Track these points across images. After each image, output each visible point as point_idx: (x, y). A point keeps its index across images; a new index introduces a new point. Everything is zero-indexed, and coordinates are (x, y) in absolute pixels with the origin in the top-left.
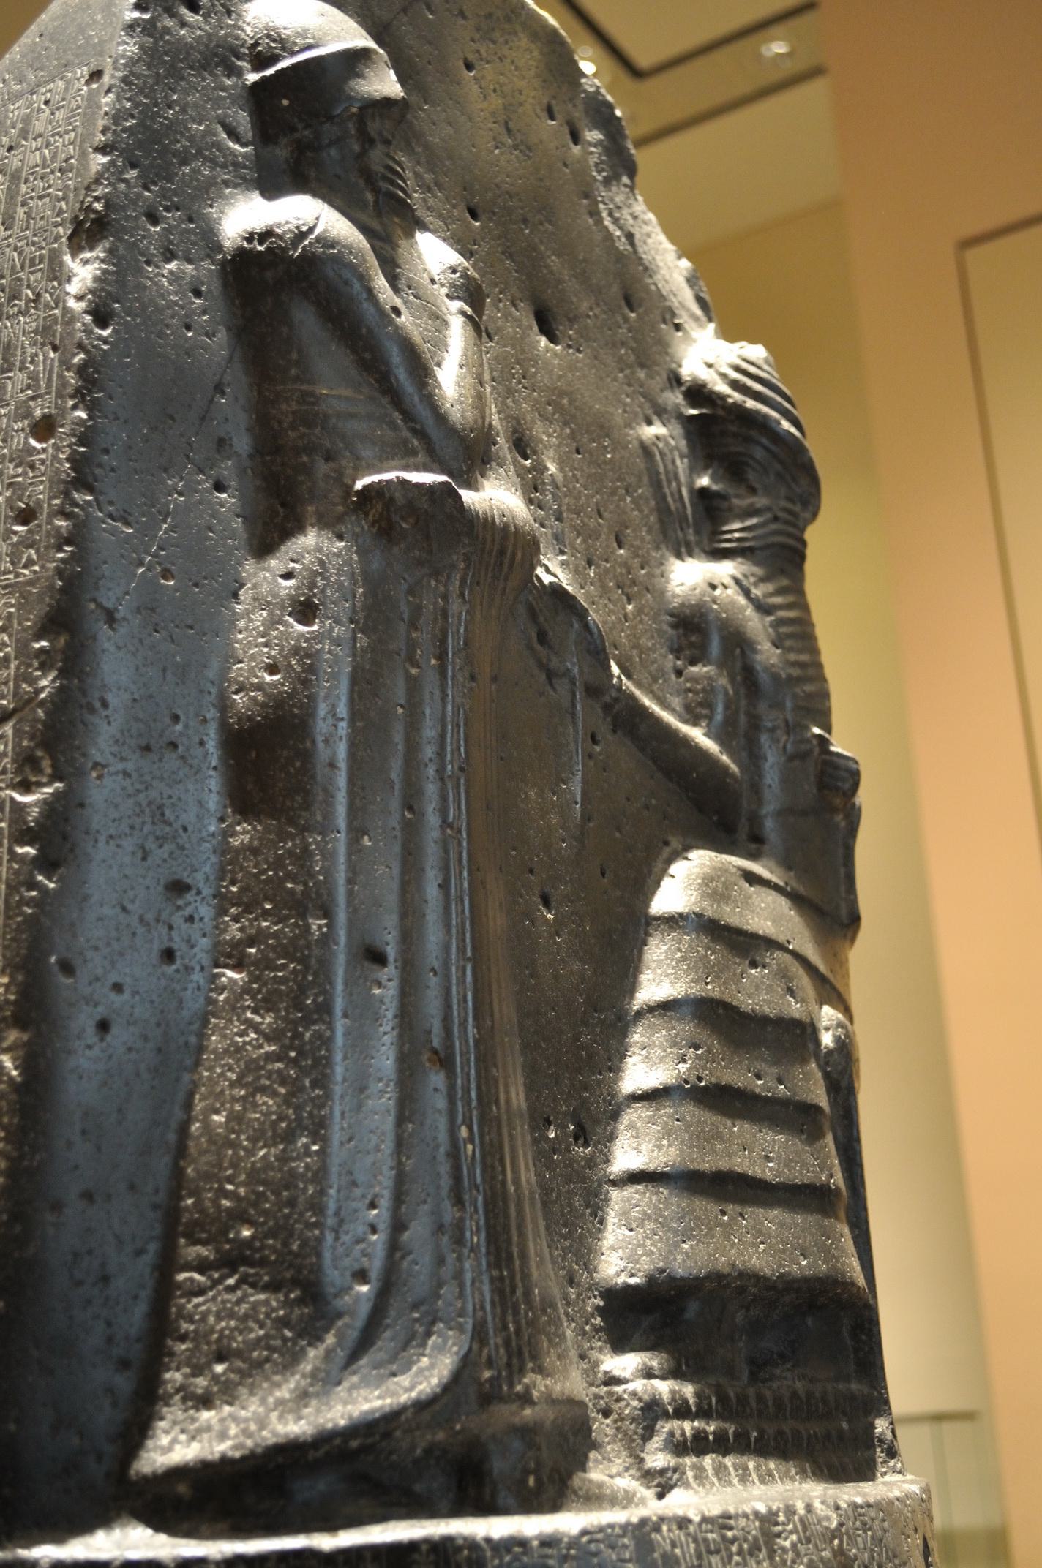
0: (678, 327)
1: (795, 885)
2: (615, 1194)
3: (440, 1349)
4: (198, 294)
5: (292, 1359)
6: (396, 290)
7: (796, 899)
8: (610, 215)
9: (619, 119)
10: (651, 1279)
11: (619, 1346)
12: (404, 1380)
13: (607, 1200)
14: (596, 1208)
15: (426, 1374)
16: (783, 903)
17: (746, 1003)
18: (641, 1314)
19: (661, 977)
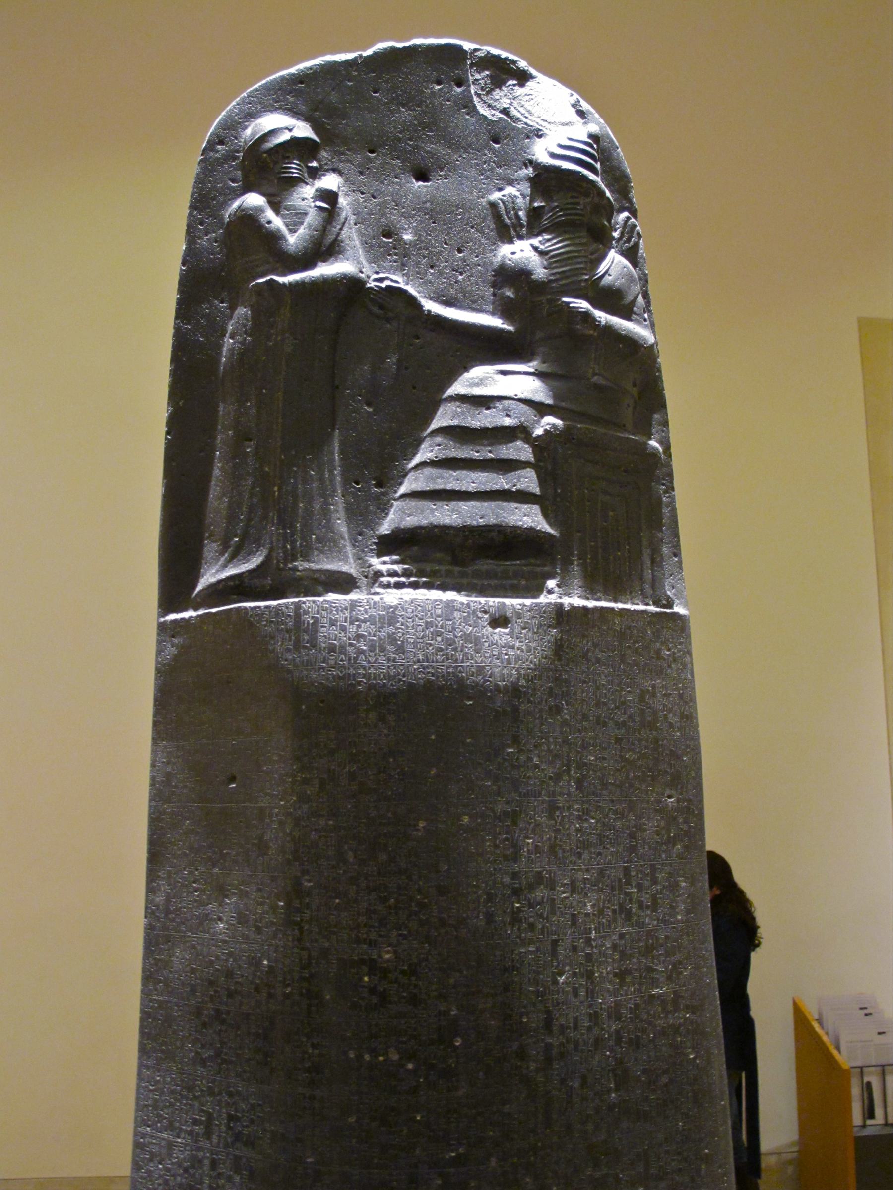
0: (540, 137)
1: (544, 368)
2: (395, 503)
3: (260, 555)
4: (216, 242)
5: (218, 560)
6: (277, 211)
7: (538, 374)
8: (489, 106)
9: (506, 59)
10: (393, 531)
11: (379, 556)
12: (246, 565)
13: (392, 505)
14: (384, 509)
15: (254, 562)
16: (531, 378)
17: (476, 424)
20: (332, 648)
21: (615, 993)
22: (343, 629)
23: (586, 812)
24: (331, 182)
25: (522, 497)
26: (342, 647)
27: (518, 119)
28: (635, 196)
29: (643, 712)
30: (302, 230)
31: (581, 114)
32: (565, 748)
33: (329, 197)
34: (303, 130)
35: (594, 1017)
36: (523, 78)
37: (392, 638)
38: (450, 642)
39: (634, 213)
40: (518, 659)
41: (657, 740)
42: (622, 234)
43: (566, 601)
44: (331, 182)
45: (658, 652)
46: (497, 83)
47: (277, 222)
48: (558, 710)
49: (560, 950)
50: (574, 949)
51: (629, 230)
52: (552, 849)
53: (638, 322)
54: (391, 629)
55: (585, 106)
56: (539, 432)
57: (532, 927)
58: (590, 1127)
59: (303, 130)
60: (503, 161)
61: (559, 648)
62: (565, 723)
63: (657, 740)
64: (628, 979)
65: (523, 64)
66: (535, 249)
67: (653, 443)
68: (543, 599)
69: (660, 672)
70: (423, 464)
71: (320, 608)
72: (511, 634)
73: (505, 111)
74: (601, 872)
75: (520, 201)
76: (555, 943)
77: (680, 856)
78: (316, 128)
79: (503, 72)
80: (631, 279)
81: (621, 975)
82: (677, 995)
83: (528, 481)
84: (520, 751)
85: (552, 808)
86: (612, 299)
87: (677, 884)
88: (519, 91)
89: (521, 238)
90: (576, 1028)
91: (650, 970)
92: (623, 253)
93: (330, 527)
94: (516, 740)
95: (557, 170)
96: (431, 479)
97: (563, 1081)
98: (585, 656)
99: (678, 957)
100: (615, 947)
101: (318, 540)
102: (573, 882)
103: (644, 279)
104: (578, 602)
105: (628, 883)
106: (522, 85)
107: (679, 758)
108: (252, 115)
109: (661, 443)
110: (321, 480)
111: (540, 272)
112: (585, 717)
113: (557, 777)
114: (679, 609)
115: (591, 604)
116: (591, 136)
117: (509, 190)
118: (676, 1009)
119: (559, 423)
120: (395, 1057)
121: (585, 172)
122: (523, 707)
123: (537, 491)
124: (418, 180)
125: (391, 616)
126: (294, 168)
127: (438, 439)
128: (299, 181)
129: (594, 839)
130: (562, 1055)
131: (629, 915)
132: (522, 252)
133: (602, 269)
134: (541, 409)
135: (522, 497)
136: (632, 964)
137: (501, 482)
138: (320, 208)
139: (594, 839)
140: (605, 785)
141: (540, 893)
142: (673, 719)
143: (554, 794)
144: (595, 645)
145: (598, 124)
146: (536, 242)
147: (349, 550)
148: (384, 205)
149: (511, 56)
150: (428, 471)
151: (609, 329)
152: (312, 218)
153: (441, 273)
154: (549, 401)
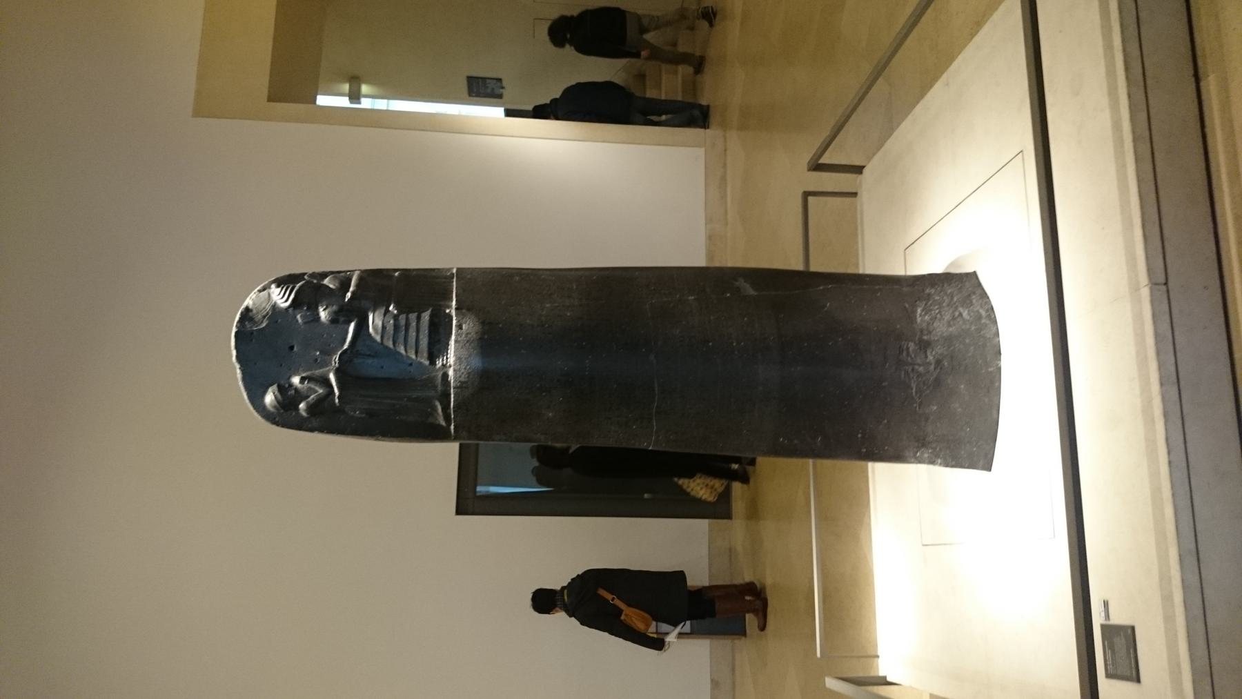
7: (374, 312)
14: (421, 363)
18: (432, 358)
19: (390, 344)
24: (296, 380)
25: (419, 318)
33: (302, 380)
46: (251, 319)
51: (313, 275)
61: (468, 310)
80: (335, 278)
83: (413, 316)
103: (332, 273)
104: (454, 303)
108: (264, 406)
111: (335, 308)
125: (459, 359)
128: (296, 390)
135: (419, 318)
137: (414, 324)
151: (357, 286)
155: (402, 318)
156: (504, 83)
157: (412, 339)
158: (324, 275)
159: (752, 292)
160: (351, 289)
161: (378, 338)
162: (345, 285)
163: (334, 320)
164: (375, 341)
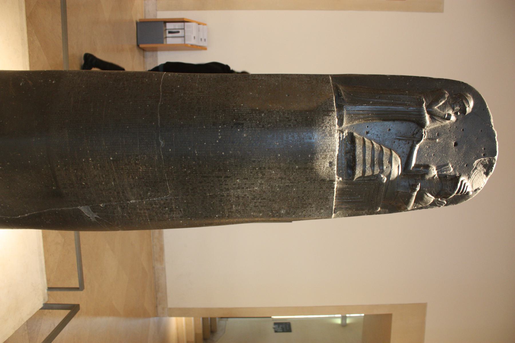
8: (477, 164)
17: (384, 159)
20: (323, 120)
21: (234, 195)
22: (328, 123)
23: (280, 188)
24: (453, 118)
25: (364, 172)
26: (323, 123)
27: (473, 171)
28: (451, 207)
29: (306, 204)
30: (439, 110)
31: (476, 190)
32: (297, 182)
33: (449, 118)
34: (469, 110)
35: (228, 189)
36: (487, 174)
37: (326, 135)
38: (325, 151)
39: (446, 205)
40: (321, 169)
41: (299, 208)
42: (440, 201)
43: (336, 183)
44: (453, 118)
45: (322, 209)
46: (485, 166)
47: (441, 104)
48: (307, 180)
49: (245, 180)
50: (245, 184)
51: (441, 204)
52: (271, 178)
53: (414, 205)
54: (328, 135)
55: (479, 191)
56: (382, 176)
57: (251, 173)
58: (201, 188)
59: (469, 110)
60: (461, 168)
61: (323, 180)
62: (304, 182)
63: (299, 208)
64: (237, 199)
65: (491, 174)
66: (434, 176)
67: (379, 209)
68: (336, 176)
69: (317, 209)
70: (373, 144)
71: (333, 117)
72: (327, 167)
73: (476, 168)
74: (264, 192)
75: (449, 172)
76: (247, 179)
77: (268, 214)
78: (469, 114)
79: (488, 168)
81: (238, 197)
82: (232, 212)
83: (368, 173)
84: (297, 170)
85: (282, 178)
86: (420, 198)
87: (260, 213)
88: (482, 173)
89: (438, 172)
90: (226, 184)
91: (239, 205)
92: (434, 201)
93: (355, 120)
94: (299, 168)
95: (458, 182)
96: (369, 147)
97: (212, 181)
98: (321, 188)
99: (242, 212)
100: (245, 195)
101: (352, 116)
102: (262, 184)
103: (426, 208)
104: (336, 186)
105: (262, 199)
106: (484, 173)
107: (294, 214)
109: (380, 211)
110: (368, 117)
111: (427, 177)
112: (305, 188)
113: (289, 180)
114: (333, 215)
115: (335, 190)
116: (468, 192)
117: (452, 170)
118: (229, 212)
119: (385, 182)
120: (220, 137)
121: (457, 190)
122: (308, 170)
123: (366, 175)
124: (455, 143)
125: (331, 135)
126: (457, 108)
127: (380, 149)
128: (453, 109)
129: (273, 190)
130: (219, 181)
131: (253, 199)
132: (434, 172)
133: (428, 194)
134: (388, 176)
135: (364, 172)
136: (241, 200)
137: (368, 166)
138: (445, 115)
139: (273, 190)
140: (287, 193)
141: (260, 175)
142: (304, 213)
143: (285, 179)
144: (324, 191)
145: (472, 195)
146: (436, 176)
147: (349, 125)
148: (447, 133)
149: (493, 170)
150: (371, 145)
151: (411, 196)
152: (442, 113)
153: (427, 149)
154: (391, 179)
155: (377, 171)
156: (273, 330)
157: (368, 152)
158: (433, 204)
159: (82, 208)
160: (416, 193)
161: (394, 154)
162: (420, 198)
163: (427, 167)
164: (396, 152)
